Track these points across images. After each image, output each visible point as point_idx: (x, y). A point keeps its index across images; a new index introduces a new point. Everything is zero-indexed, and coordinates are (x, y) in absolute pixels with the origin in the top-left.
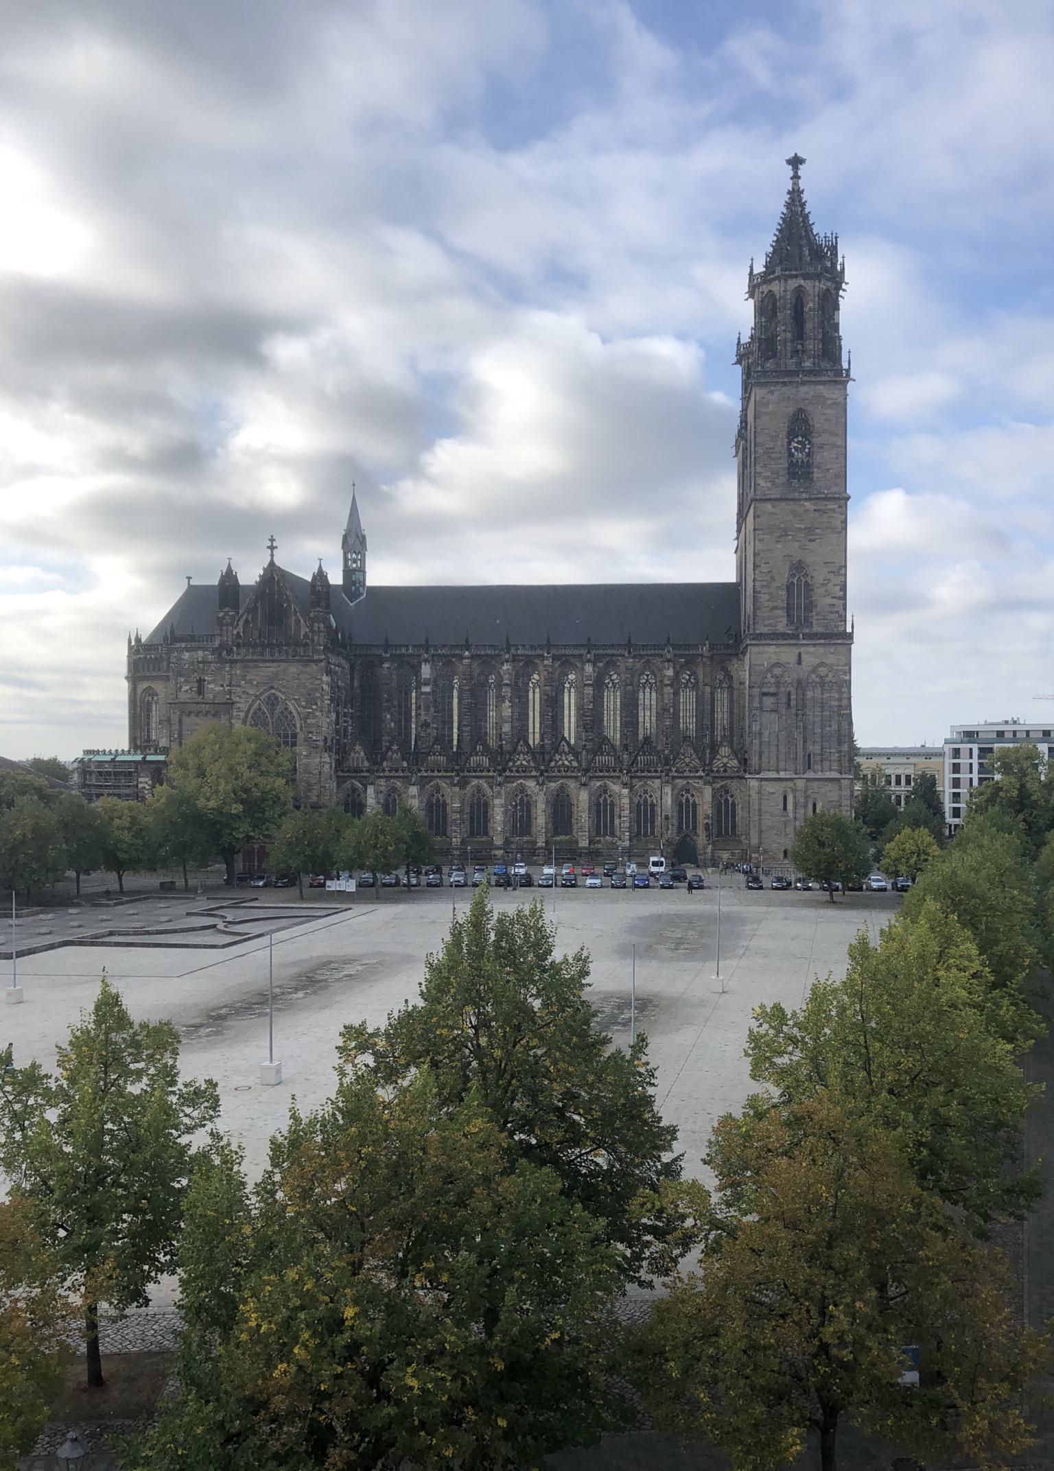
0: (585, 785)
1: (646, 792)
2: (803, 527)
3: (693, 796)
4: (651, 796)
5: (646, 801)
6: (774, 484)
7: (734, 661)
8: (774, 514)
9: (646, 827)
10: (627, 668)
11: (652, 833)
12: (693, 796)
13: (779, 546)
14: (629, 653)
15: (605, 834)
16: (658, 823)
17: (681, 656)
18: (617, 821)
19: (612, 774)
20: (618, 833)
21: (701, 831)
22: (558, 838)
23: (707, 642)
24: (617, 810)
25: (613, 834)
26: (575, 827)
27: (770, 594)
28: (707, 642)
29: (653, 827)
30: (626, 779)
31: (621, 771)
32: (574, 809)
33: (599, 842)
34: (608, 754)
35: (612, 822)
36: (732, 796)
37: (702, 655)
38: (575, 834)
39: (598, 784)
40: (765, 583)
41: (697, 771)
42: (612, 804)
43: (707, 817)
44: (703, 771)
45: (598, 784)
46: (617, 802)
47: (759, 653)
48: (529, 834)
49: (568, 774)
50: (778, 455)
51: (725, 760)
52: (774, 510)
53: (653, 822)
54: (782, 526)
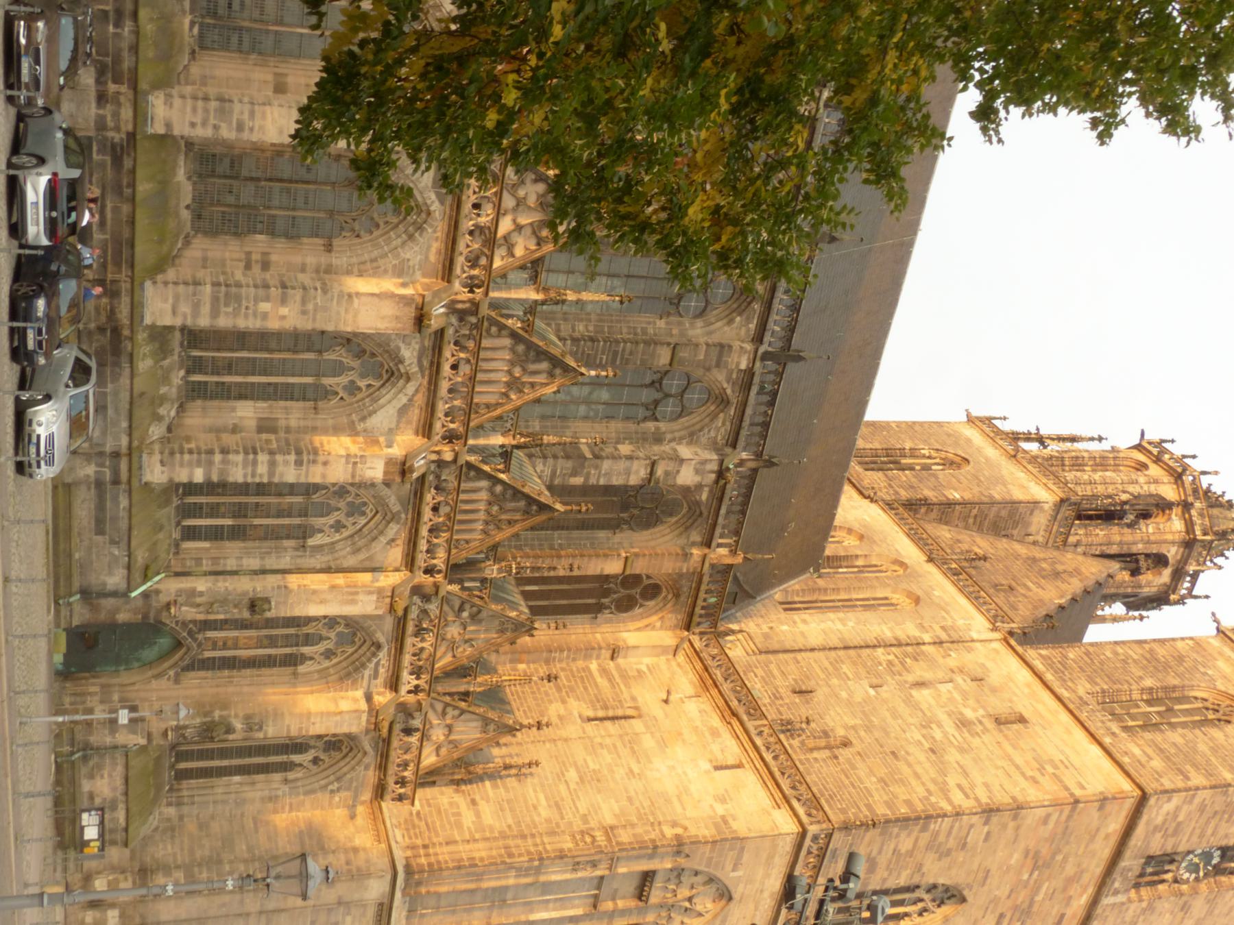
0: (420, 320)
1: (355, 510)
2: (1039, 898)
3: (328, 654)
4: (338, 526)
5: (326, 511)
6: (1157, 829)
7: (673, 618)
8: (1093, 838)
9: (214, 511)
10: (723, 349)
11: (191, 534)
12: (328, 654)
13: (1016, 857)
14: (766, 356)
15: (196, 366)
16: (233, 554)
17: (719, 496)
18: (247, 412)
19: (441, 407)
20: (199, 418)
21: (198, 685)
22: (181, 175)
23: (739, 559)
24: (292, 414)
25: (196, 392)
26: (228, 251)
27: (910, 853)
28: (739, 559)
29: (216, 534)
30: (419, 464)
31: (450, 437)
32: (310, 254)
33: (163, 350)
34: (514, 384)
35: (245, 394)
36: (316, 761)
37: (708, 544)
38: (200, 246)
39: (409, 354)
40: (942, 838)
41: (417, 672)
42: (316, 395)
43: (252, 724)
44: (416, 690)
45: (409, 354)
46: (330, 411)
47: (771, 857)
48: (203, 44)
49: (467, 245)
50: (1210, 831)
51: (438, 734)
52: (1102, 834)
53: (237, 533)
54: (1059, 858)
